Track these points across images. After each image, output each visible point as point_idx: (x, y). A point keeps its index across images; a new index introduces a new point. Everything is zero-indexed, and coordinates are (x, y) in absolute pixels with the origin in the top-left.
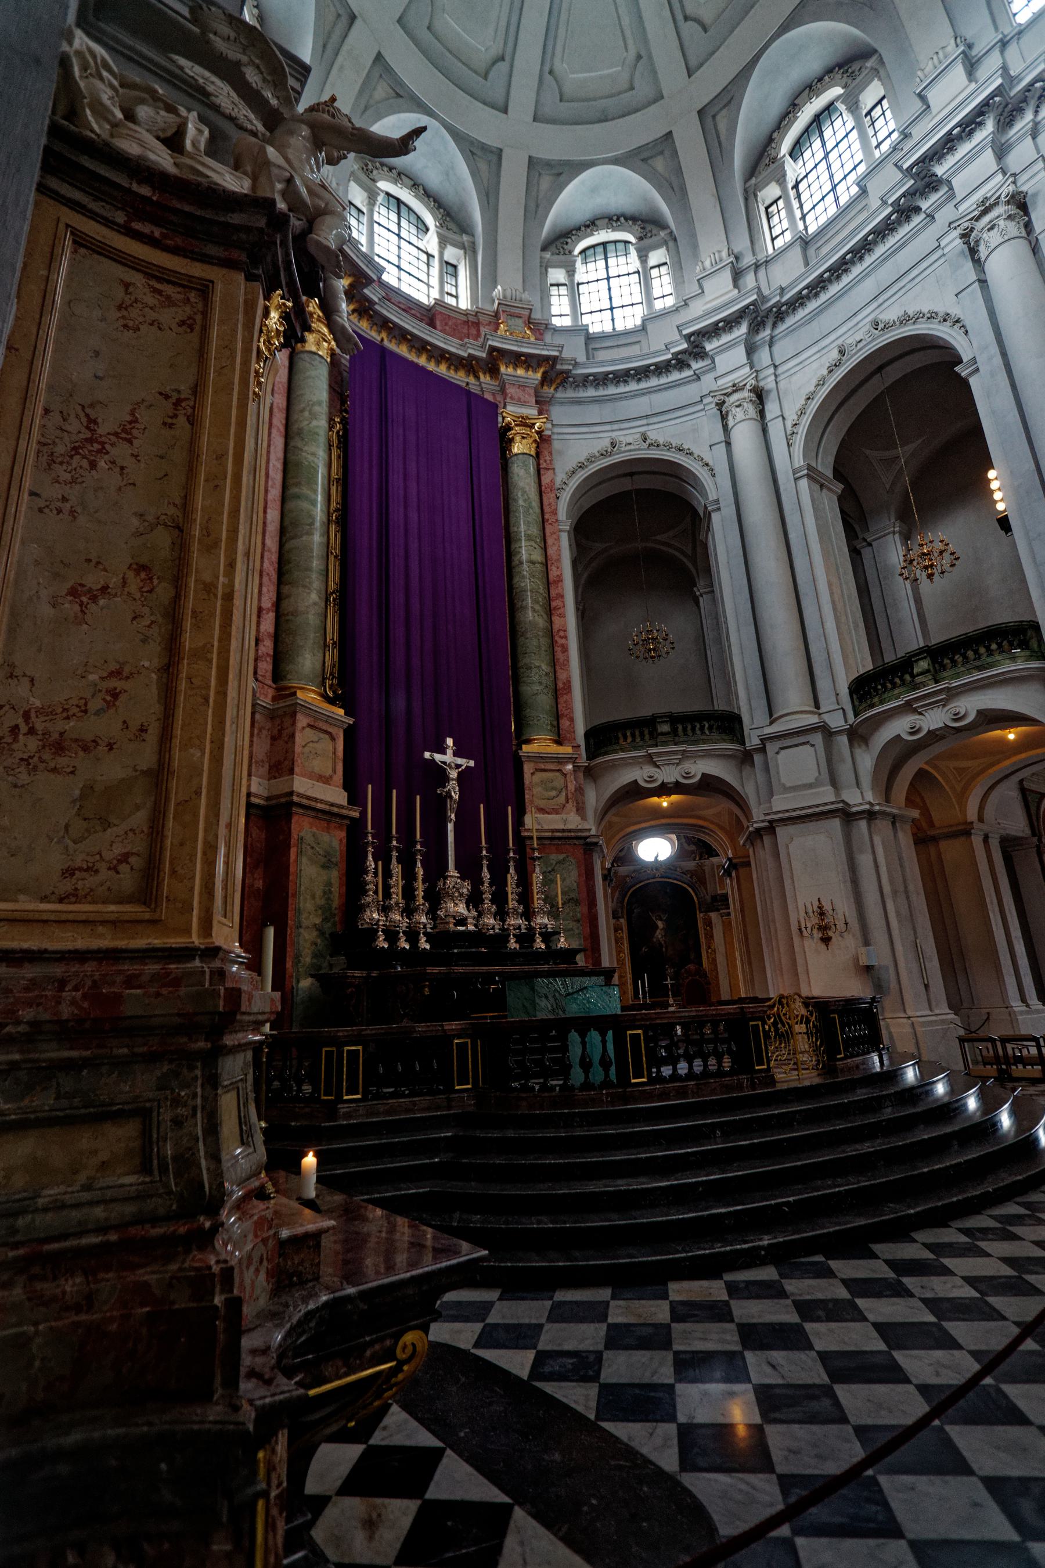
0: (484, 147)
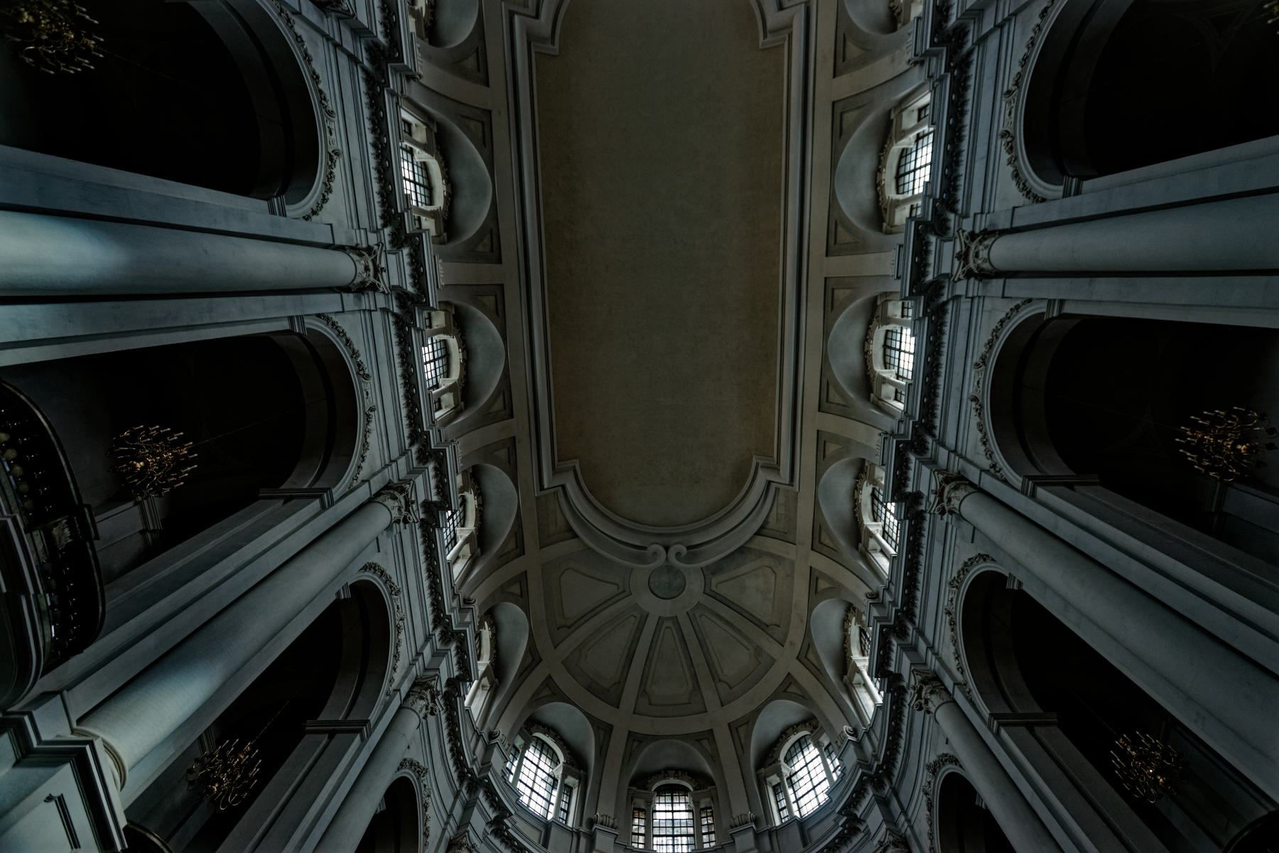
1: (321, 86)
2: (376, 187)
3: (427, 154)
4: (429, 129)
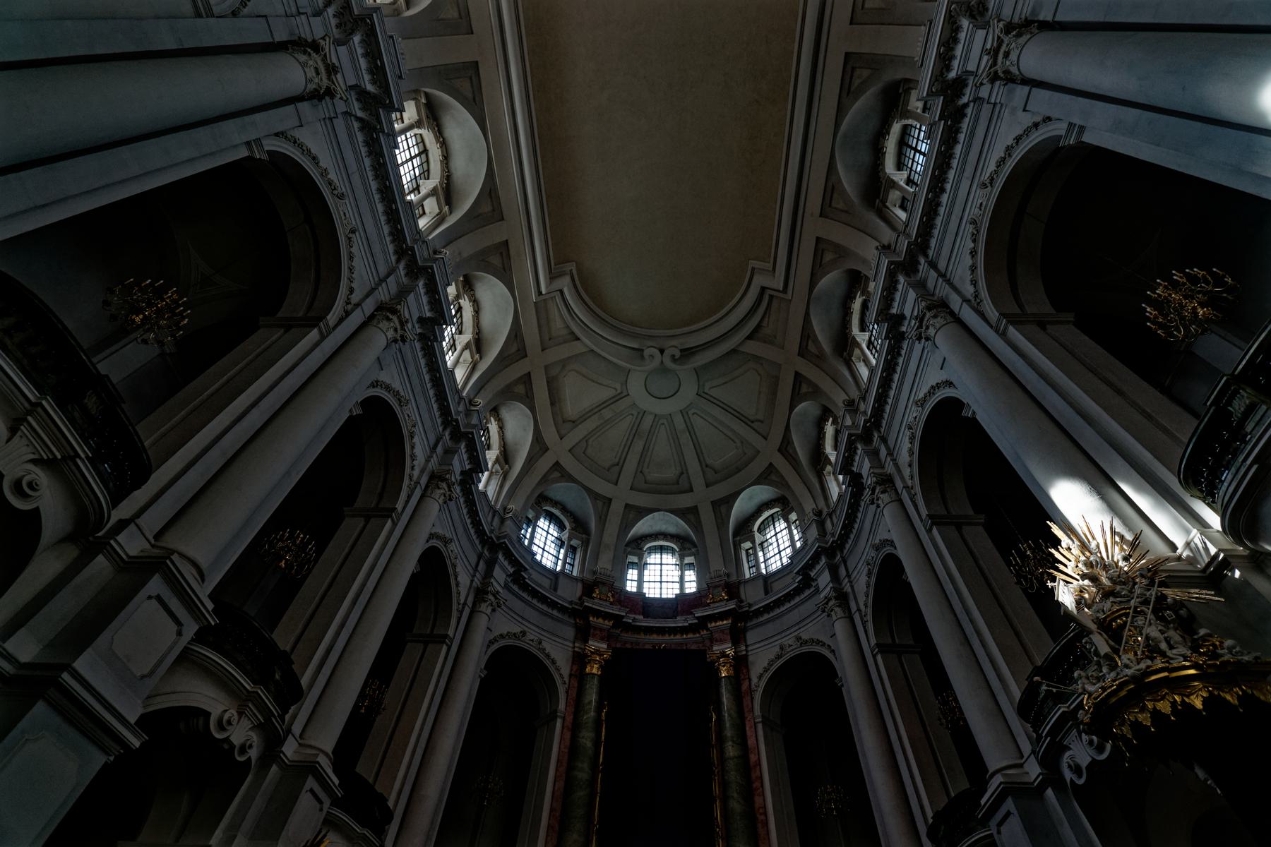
0: (688, 509)
1: (972, 245)
2: (958, 149)
3: (894, 178)
4: (884, 202)
